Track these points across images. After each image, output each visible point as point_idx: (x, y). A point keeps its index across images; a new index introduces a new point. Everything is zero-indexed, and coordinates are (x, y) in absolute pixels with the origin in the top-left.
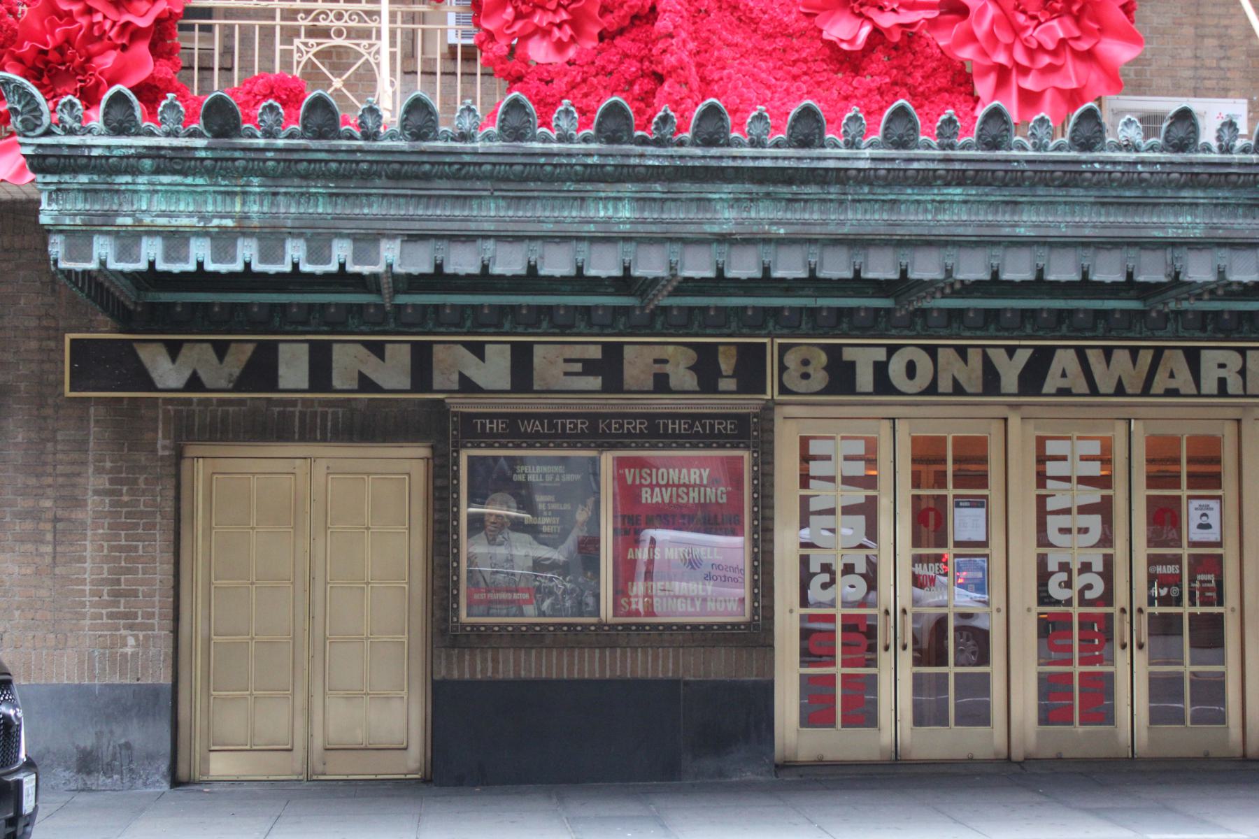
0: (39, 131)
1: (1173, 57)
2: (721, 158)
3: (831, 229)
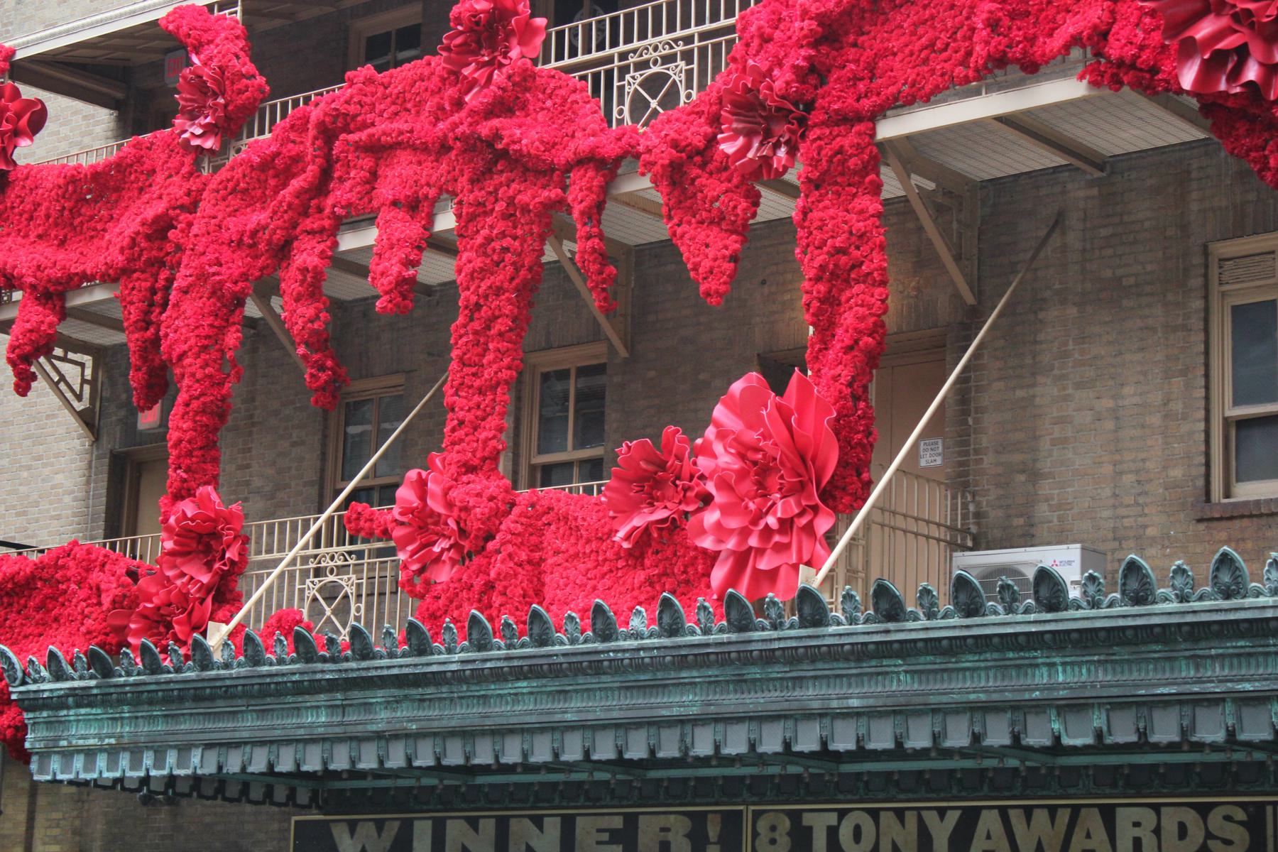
0: (17, 682)
1: (1093, 498)
2: (368, 669)
3: (444, 723)
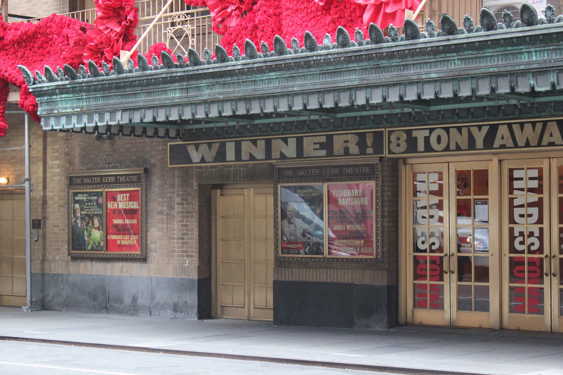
0: (31, 83)
2: (198, 70)
3: (236, 94)
